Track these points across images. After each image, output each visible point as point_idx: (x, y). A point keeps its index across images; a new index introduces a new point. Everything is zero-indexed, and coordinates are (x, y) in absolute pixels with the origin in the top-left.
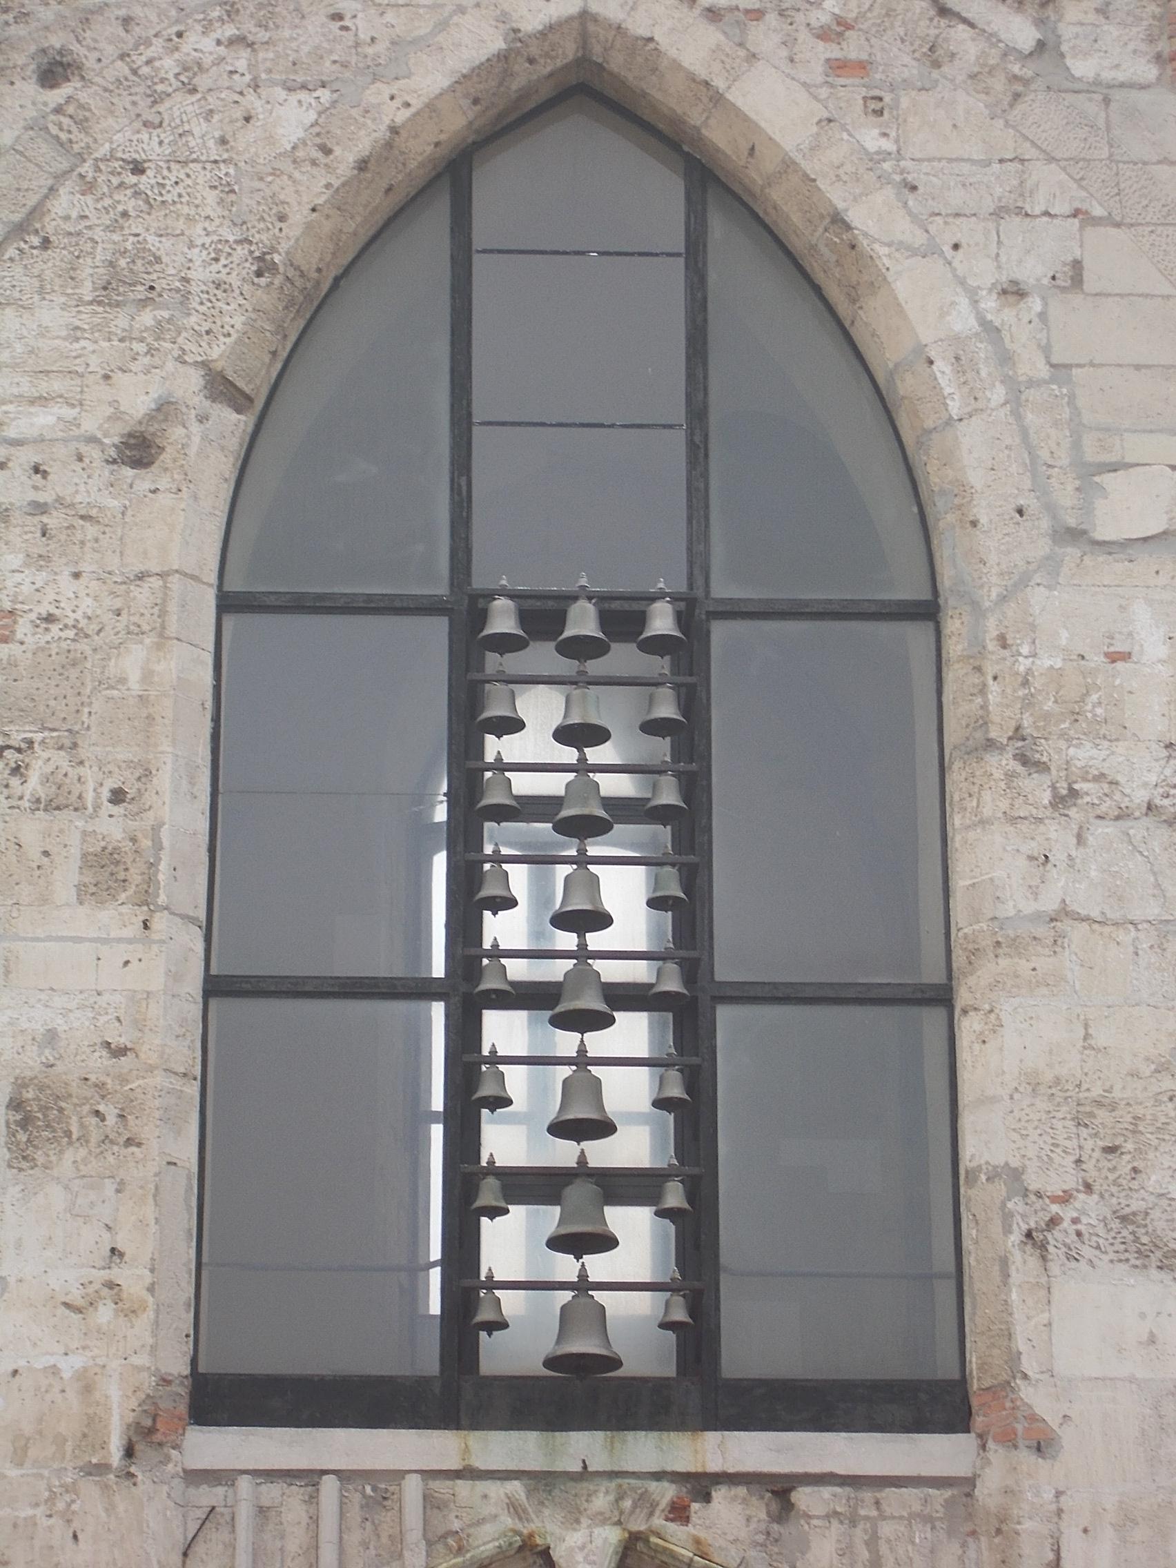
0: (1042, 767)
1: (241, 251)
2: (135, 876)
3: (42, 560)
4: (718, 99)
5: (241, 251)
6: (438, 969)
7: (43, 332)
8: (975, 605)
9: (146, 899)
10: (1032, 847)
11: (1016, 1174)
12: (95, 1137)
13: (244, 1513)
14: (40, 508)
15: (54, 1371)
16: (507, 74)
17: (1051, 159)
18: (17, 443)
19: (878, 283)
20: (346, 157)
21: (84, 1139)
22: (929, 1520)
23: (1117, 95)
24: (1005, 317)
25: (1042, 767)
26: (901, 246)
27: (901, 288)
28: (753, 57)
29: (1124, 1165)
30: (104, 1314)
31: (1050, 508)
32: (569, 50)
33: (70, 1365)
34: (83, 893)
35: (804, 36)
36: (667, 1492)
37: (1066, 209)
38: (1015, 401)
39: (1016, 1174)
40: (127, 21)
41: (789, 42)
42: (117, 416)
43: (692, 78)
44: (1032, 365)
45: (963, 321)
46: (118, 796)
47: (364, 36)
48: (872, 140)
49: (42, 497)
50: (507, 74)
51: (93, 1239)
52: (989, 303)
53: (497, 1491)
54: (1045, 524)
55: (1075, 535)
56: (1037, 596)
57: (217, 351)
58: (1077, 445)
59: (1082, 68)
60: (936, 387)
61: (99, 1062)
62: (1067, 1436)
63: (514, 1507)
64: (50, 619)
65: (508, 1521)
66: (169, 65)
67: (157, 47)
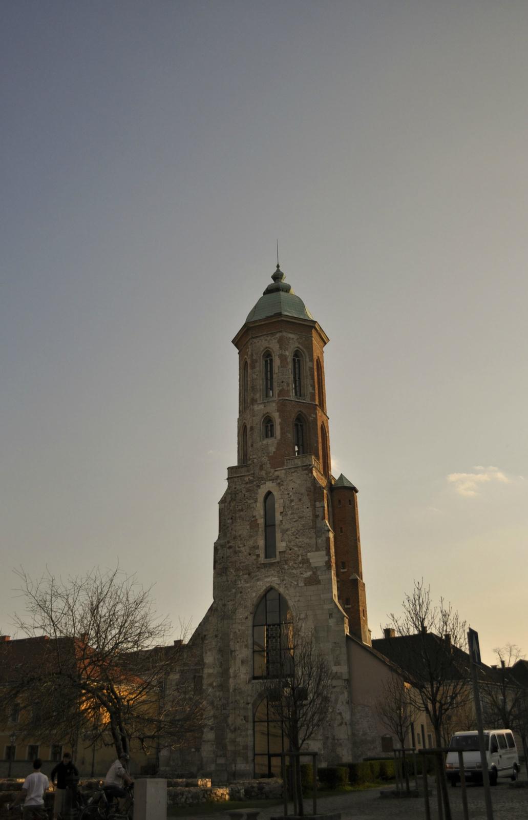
20: (257, 597)
57: (251, 611)
59: (300, 585)
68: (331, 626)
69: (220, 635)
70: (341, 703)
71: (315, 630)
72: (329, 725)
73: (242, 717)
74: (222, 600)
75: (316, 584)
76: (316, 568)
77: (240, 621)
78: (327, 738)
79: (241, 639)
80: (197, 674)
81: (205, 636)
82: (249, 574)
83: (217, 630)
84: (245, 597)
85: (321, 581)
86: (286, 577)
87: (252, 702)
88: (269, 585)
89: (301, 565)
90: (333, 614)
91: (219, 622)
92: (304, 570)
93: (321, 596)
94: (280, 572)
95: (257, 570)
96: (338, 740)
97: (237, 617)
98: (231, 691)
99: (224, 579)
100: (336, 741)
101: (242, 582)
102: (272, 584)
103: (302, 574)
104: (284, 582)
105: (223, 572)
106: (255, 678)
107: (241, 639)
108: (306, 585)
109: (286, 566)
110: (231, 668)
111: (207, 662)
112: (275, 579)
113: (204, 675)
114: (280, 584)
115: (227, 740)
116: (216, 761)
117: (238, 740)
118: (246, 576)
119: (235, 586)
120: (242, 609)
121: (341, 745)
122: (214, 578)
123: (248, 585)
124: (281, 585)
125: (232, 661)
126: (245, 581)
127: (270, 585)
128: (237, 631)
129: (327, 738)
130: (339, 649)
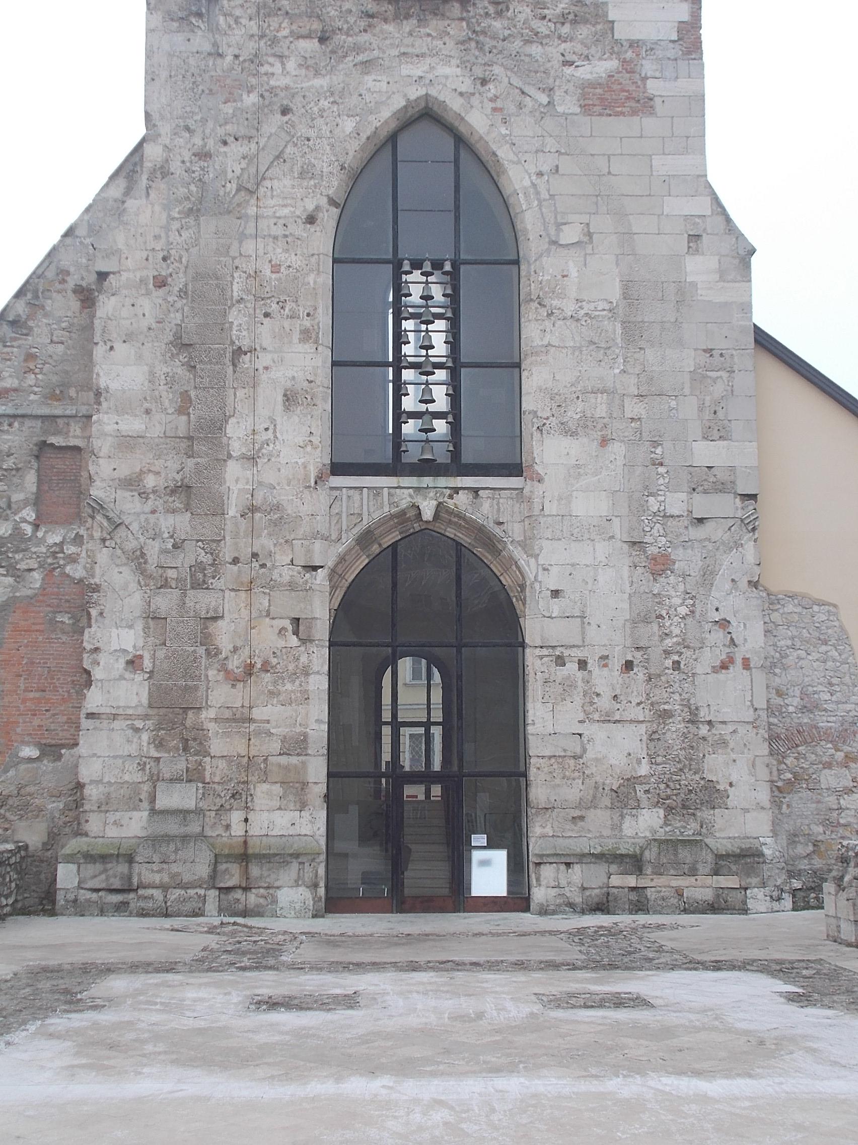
0: (545, 306)
1: (336, 163)
2: (313, 336)
3: (287, 251)
4: (462, 119)
5: (336, 163)
6: (391, 359)
7: (285, 187)
8: (528, 262)
9: (316, 342)
10: (542, 327)
11: (536, 412)
12: (305, 404)
13: (344, 497)
14: (286, 236)
15: (297, 463)
16: (406, 112)
17: (551, 136)
18: (279, 218)
19: (505, 172)
20: (364, 137)
21: (302, 404)
22: (512, 498)
23: (569, 117)
24: (537, 181)
25: (545, 306)
26: (511, 161)
27: (511, 173)
28: (472, 107)
29: (562, 410)
30: (309, 448)
31: (548, 235)
32: (423, 105)
33: (300, 461)
34: (300, 341)
35: (485, 100)
36: (448, 492)
37: (553, 150)
38: (540, 205)
39: (536, 412)
40: (304, 97)
41: (482, 102)
42: (305, 210)
43: (455, 113)
44: (544, 195)
45: (527, 183)
46: (308, 315)
47: (368, 101)
48: (504, 131)
49: (287, 233)
50: (406, 112)
51: (305, 430)
52: (534, 177)
53: (406, 491)
54: (547, 240)
55: (554, 243)
56: (544, 259)
57: (331, 192)
58: (556, 217)
59: (560, 109)
60: (519, 201)
61: (306, 384)
62: (546, 478)
63: (410, 496)
64: (289, 267)
65: (409, 499)
66: (316, 109)
67: (312, 104)
68: (694, 285)
69: (179, 281)
70: (728, 586)
71: (625, 296)
72: (676, 665)
73: (287, 624)
74: (187, 129)
75: (634, 113)
76: (634, 44)
77: (279, 231)
78: (667, 715)
79: (282, 304)
80: (53, 440)
81: (102, 276)
82: (322, 40)
83: (165, 259)
84: (303, 130)
85: (658, 101)
86: (497, 69)
87: (330, 563)
88: (422, 92)
89: (566, 30)
90: (705, 238)
91: (176, 225)
92: (579, 48)
93: (656, 161)
94: (473, 44)
95: (362, 24)
96: (710, 723)
97: (270, 212)
98: (232, 512)
99: (201, 41)
100: (704, 730)
101: (291, 65)
102: (433, 92)
103: (571, 63)
104: (491, 86)
105: (199, 15)
106: (338, 469)
107: (282, 304)
108: (586, 109)
109: (497, 24)
110: (232, 421)
111: (114, 386)
112: (447, 71)
113: (96, 443)
114: (473, 94)
115: (212, 713)
116: (153, 799)
117: (256, 714)
118: (309, 46)
119: (253, 81)
120: (287, 182)
121: (724, 743)
122: (150, 31)
123: (321, 82)
124: (475, 101)
125: (240, 393)
126: (304, 64)
127: (427, 94)
128: (267, 271)
129: (667, 715)
130: (724, 374)
